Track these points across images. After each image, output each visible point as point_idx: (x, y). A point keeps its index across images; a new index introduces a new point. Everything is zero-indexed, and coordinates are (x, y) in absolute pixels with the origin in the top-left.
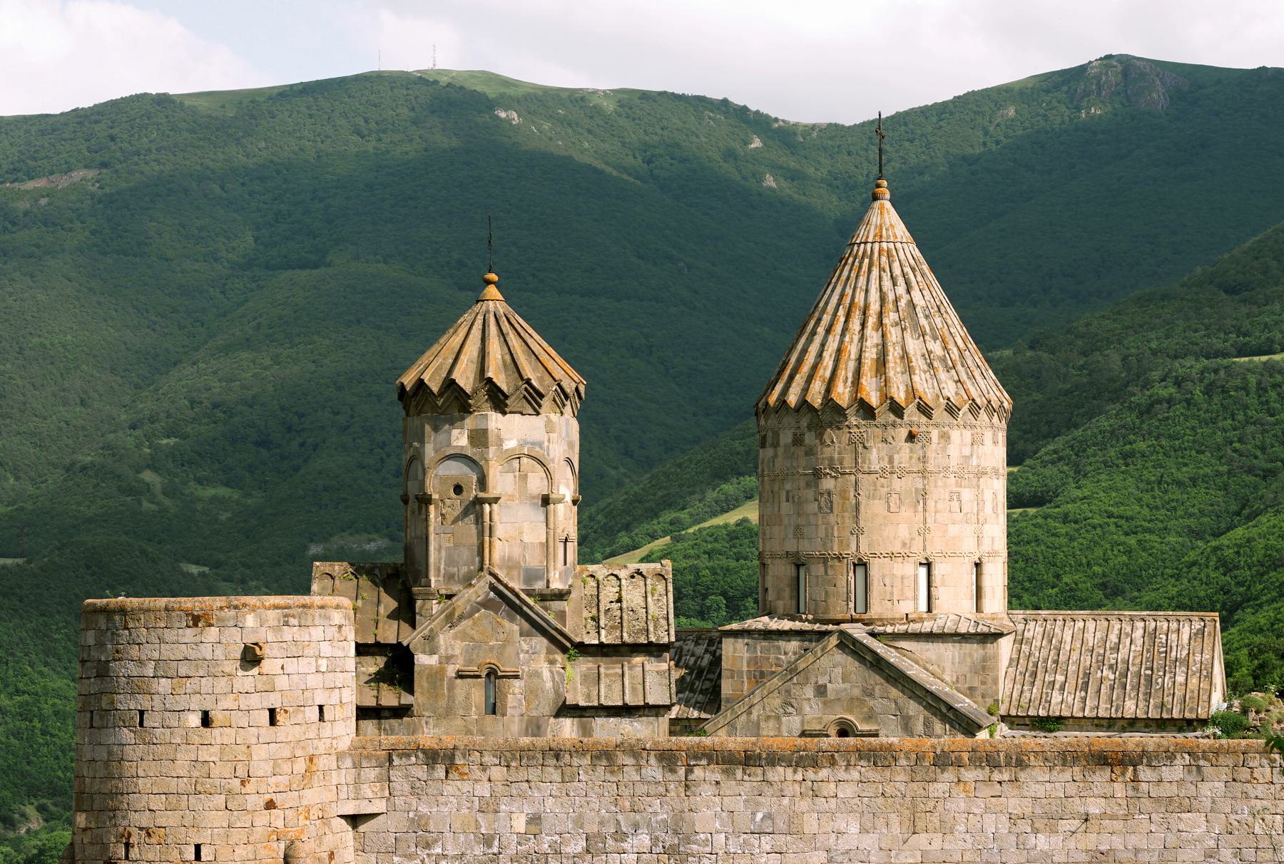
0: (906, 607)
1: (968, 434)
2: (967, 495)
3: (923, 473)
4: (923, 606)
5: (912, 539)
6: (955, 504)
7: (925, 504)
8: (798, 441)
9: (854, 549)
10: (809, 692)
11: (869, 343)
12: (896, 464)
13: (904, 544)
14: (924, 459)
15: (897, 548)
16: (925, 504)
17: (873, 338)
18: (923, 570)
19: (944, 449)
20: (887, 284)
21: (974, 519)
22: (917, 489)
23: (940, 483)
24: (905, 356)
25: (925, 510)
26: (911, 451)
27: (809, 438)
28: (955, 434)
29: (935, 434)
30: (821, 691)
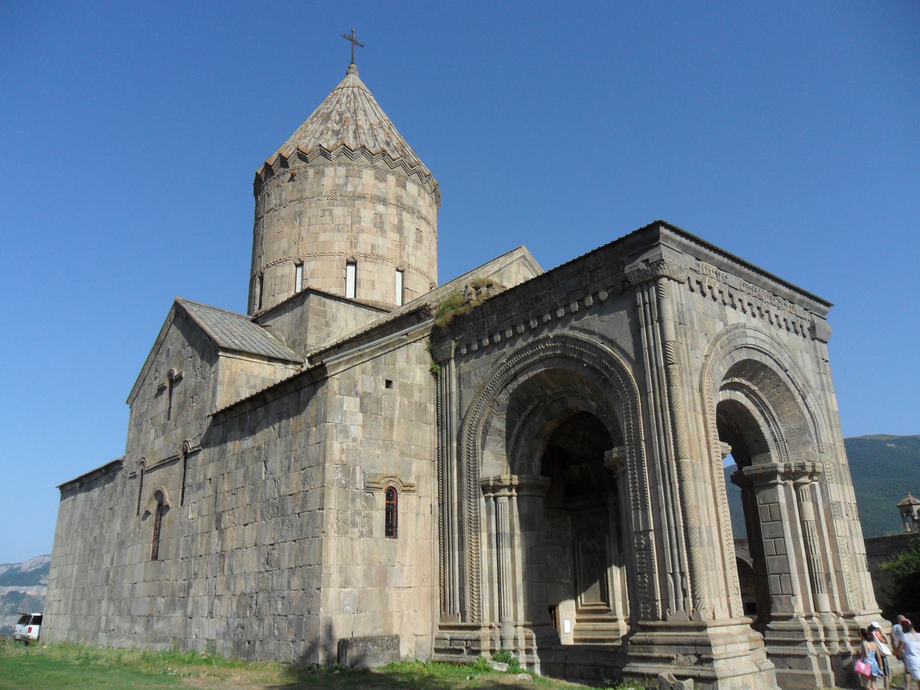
1: (342, 171)
3: (300, 200)
5: (290, 247)
6: (327, 218)
7: (300, 221)
12: (283, 198)
13: (284, 252)
14: (301, 191)
15: (280, 256)
16: (300, 221)
19: (319, 181)
22: (295, 212)
23: (313, 205)
25: (300, 224)
26: (293, 187)
28: (329, 171)
29: (311, 172)
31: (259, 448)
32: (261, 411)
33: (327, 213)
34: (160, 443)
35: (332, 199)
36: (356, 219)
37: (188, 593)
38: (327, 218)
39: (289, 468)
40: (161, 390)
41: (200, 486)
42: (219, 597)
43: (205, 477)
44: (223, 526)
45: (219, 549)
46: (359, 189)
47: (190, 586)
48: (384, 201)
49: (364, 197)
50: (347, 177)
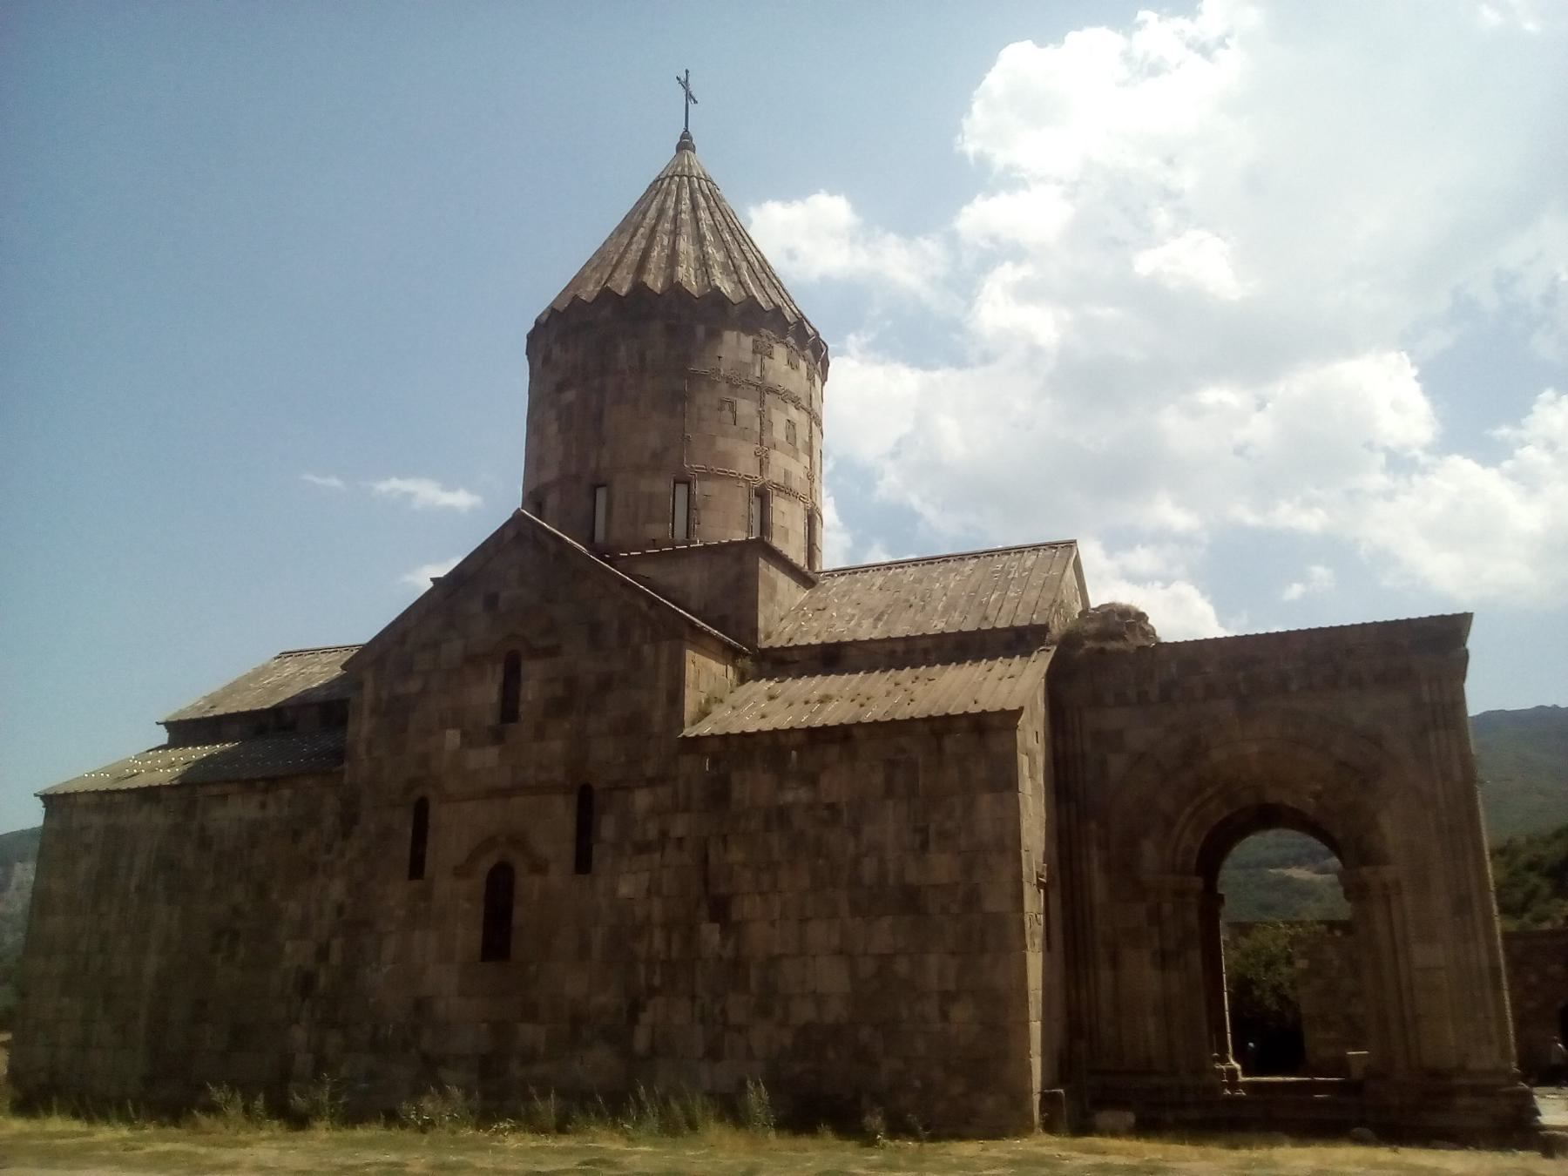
0: (655, 531)
1: (747, 341)
2: (746, 407)
4: (680, 532)
6: (727, 414)
8: (547, 360)
9: (593, 465)
10: (476, 606)
11: (634, 247)
17: (640, 243)
18: (681, 491)
20: (671, 203)
21: (756, 438)
24: (673, 258)
27: (557, 352)
28: (730, 336)
29: (701, 330)
30: (491, 601)
31: (831, 807)
32: (833, 752)
33: (727, 406)
34: (486, 758)
35: (734, 387)
36: (765, 424)
37: (633, 1019)
38: (727, 414)
39: (924, 846)
40: (473, 660)
41: (643, 848)
42: (740, 1029)
43: (664, 834)
44: (735, 917)
45: (728, 953)
46: (771, 378)
47: (634, 1009)
48: (796, 402)
49: (776, 392)
50: (754, 352)
